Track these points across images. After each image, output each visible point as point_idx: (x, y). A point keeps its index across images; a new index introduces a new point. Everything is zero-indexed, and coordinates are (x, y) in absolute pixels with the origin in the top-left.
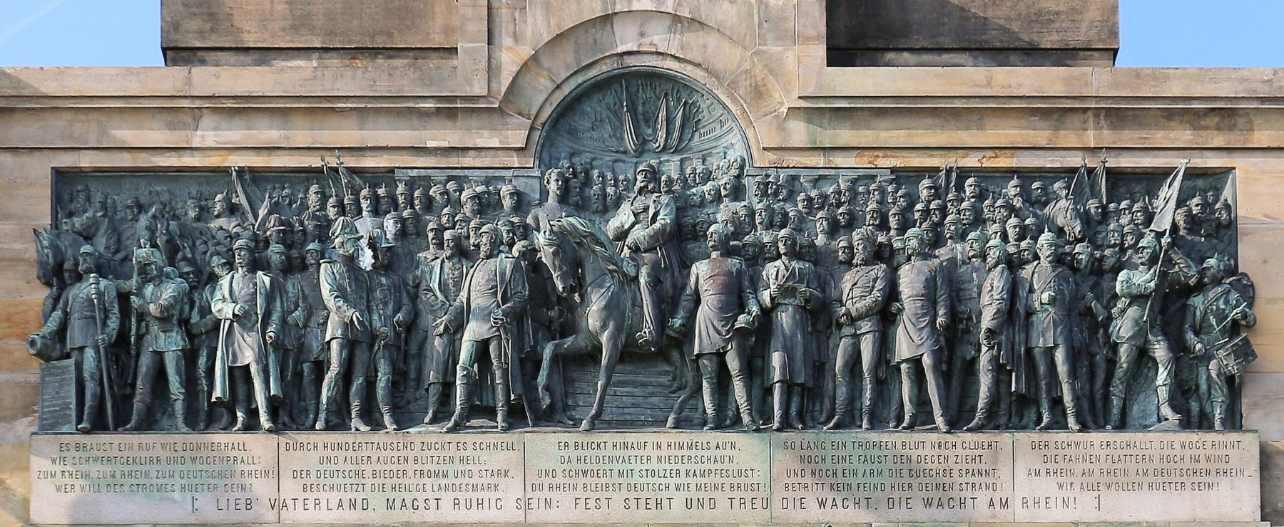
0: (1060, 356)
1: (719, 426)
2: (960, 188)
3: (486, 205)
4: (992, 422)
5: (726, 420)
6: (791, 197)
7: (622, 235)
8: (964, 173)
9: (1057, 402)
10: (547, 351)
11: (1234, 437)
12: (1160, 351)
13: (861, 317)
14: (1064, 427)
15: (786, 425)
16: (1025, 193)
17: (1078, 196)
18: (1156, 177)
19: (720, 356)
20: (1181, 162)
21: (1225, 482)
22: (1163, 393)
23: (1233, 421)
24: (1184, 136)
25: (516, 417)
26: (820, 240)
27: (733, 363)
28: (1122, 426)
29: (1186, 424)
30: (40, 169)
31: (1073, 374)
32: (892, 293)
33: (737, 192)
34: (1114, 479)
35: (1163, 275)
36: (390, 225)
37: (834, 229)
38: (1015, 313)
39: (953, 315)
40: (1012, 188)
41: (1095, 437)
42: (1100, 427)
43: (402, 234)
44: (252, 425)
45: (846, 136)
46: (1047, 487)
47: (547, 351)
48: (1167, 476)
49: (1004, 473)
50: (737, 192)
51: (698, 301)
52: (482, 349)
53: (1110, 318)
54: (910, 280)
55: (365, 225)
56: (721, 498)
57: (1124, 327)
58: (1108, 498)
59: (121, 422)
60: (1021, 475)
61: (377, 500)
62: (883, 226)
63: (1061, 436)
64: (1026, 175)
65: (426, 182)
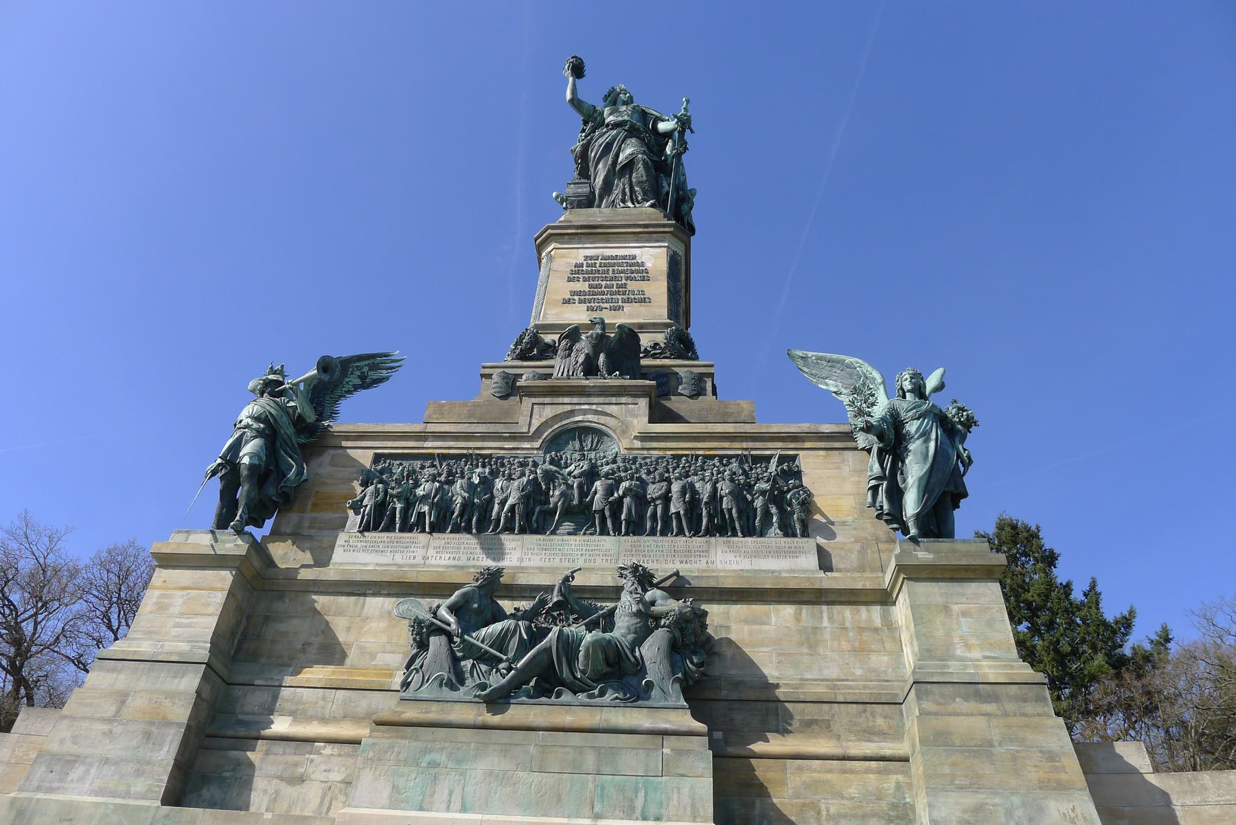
0: (734, 511)
1: (601, 534)
2: (697, 460)
3: (522, 465)
4: (709, 532)
5: (604, 532)
6: (634, 463)
7: (570, 474)
8: (697, 456)
9: (734, 529)
10: (537, 510)
11: (805, 540)
12: (774, 510)
13: (657, 498)
14: (736, 535)
15: (627, 534)
16: (721, 461)
17: (741, 463)
18: (768, 459)
19: (603, 510)
20: (780, 452)
21: (803, 556)
22: (776, 525)
23: (805, 534)
24: (779, 445)
25: (523, 531)
26: (644, 476)
27: (607, 513)
28: (762, 535)
29: (786, 535)
30: (371, 453)
31: (739, 518)
32: (669, 490)
33: (614, 462)
34: (756, 554)
35: (773, 487)
36: (487, 470)
37: (649, 473)
38: (715, 497)
39: (692, 497)
40: (716, 461)
41: (749, 539)
42: (751, 535)
43: (491, 473)
44: (423, 531)
45: (655, 445)
46: (730, 557)
47: (537, 510)
48: (779, 553)
49: (712, 552)
50: (614, 462)
51: (596, 493)
52: (513, 507)
53: (753, 501)
54: (676, 487)
55: (479, 470)
56: (599, 560)
57: (759, 503)
58: (755, 561)
59: (375, 529)
60: (719, 553)
61: (464, 558)
62: (668, 471)
63: (736, 539)
64: (721, 457)
65: (503, 458)
